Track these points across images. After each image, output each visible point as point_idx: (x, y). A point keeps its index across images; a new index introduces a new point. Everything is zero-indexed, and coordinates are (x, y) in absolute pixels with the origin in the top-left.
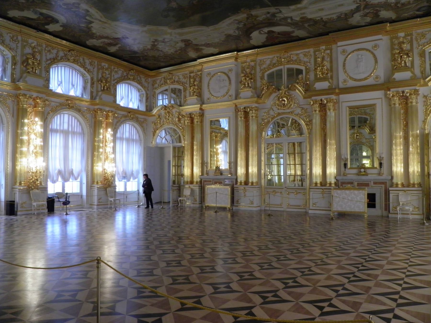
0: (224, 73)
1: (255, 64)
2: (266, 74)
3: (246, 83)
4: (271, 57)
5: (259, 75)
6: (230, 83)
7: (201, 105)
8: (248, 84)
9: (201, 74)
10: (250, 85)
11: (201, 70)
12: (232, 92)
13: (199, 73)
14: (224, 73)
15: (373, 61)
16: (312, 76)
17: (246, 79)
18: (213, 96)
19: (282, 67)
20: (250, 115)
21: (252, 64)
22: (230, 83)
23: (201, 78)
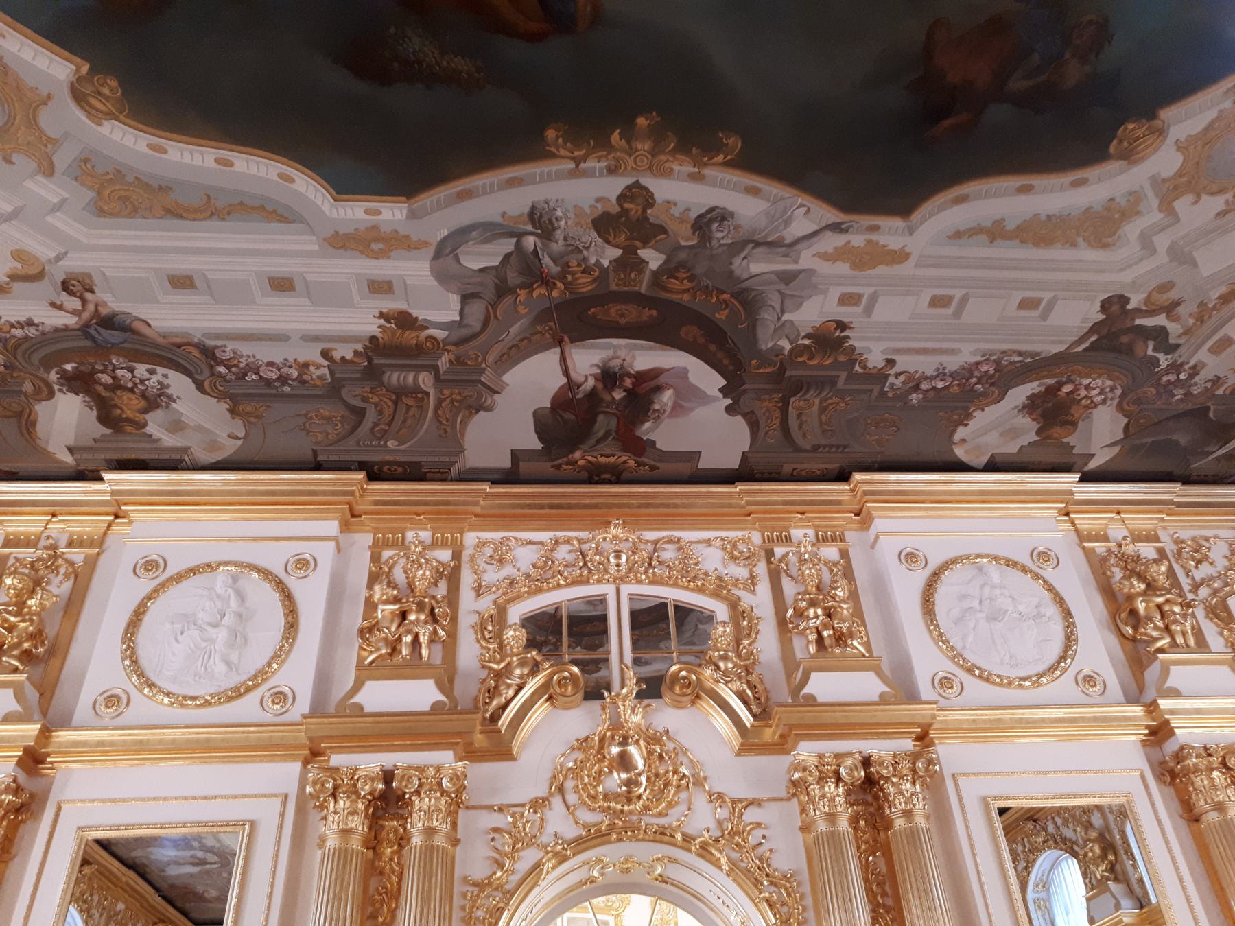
0: (266, 574)
1: (457, 556)
2: (516, 613)
3: (408, 639)
4: (545, 536)
5: (471, 606)
6: (292, 626)
7: (45, 733)
8: (416, 641)
9: (91, 564)
10: (425, 652)
11: (98, 542)
12: (298, 676)
13: (77, 555)
14: (266, 574)
15: (1052, 611)
16: (767, 644)
17: (404, 615)
18: (151, 685)
19: (608, 590)
20: (416, 826)
21: (445, 555)
22: (292, 626)
23: (82, 578)
